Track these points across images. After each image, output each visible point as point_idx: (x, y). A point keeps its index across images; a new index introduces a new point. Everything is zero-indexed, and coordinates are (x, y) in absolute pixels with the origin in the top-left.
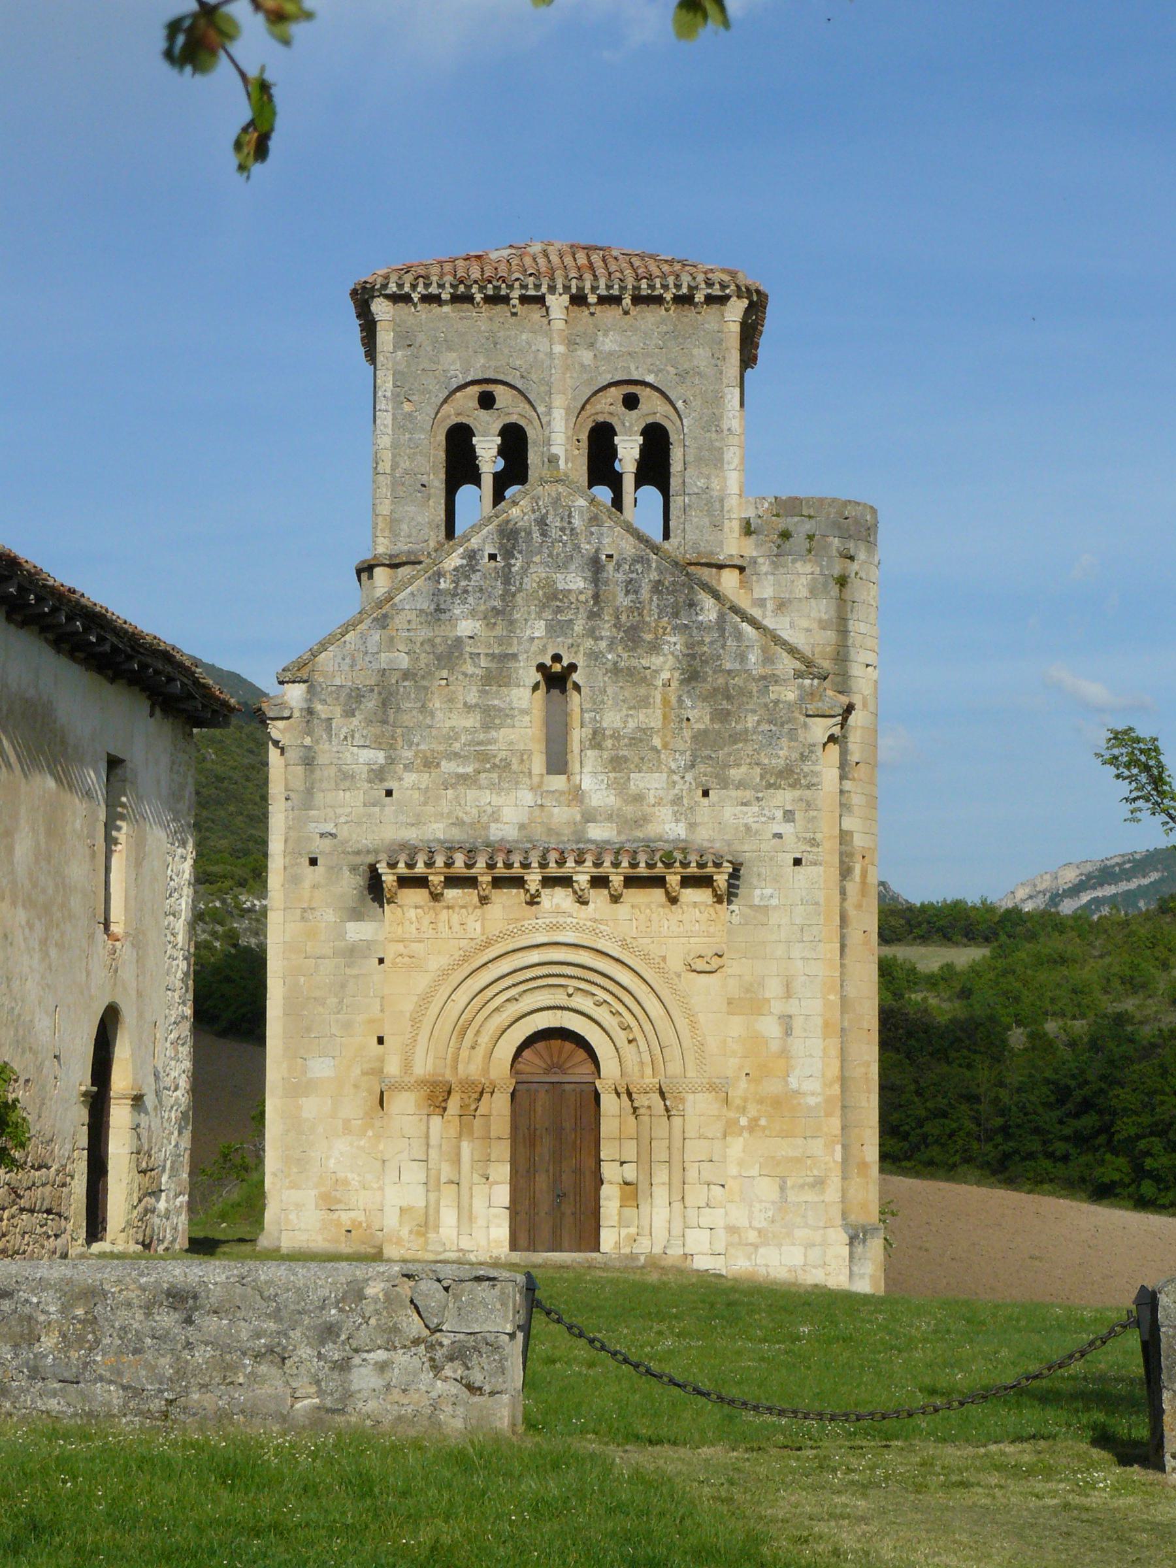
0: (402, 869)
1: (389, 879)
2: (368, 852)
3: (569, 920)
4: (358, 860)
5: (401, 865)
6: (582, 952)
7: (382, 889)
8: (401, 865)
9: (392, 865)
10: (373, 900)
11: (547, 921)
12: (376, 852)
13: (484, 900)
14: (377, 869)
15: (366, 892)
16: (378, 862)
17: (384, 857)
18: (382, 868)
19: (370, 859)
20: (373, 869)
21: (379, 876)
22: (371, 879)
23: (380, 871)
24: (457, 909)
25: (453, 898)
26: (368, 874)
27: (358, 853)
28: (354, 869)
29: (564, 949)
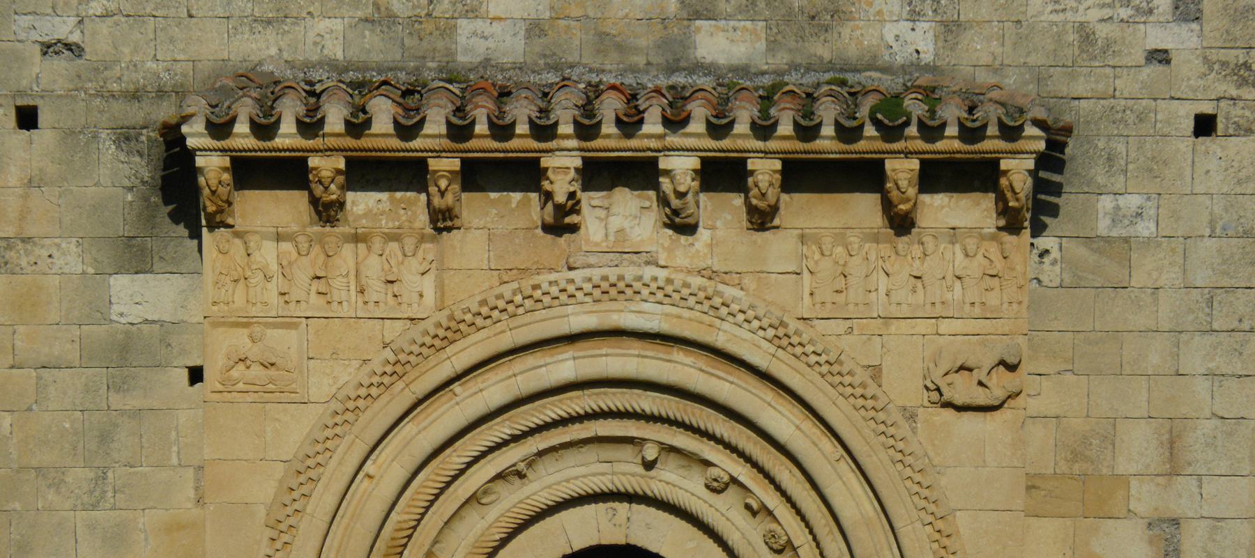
0: (242, 137)
1: (212, 165)
2: (161, 93)
3: (649, 272)
4: (136, 114)
5: (242, 127)
6: (678, 354)
7: (197, 190)
8: (242, 127)
9: (219, 129)
10: (175, 218)
11: (596, 274)
12: (181, 93)
13: (443, 221)
14: (183, 138)
15: (156, 199)
16: (185, 119)
17: (198, 106)
18: (195, 135)
19: (165, 112)
20: (172, 136)
21: (190, 155)
22: (168, 162)
23: (191, 142)
24: (377, 244)
25: (365, 215)
26: (160, 151)
27: (135, 95)
28: (125, 137)
29: (636, 347)
